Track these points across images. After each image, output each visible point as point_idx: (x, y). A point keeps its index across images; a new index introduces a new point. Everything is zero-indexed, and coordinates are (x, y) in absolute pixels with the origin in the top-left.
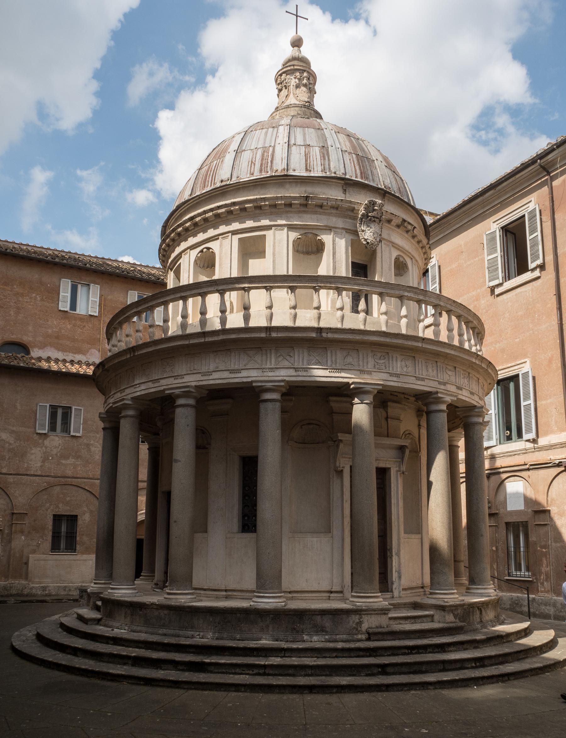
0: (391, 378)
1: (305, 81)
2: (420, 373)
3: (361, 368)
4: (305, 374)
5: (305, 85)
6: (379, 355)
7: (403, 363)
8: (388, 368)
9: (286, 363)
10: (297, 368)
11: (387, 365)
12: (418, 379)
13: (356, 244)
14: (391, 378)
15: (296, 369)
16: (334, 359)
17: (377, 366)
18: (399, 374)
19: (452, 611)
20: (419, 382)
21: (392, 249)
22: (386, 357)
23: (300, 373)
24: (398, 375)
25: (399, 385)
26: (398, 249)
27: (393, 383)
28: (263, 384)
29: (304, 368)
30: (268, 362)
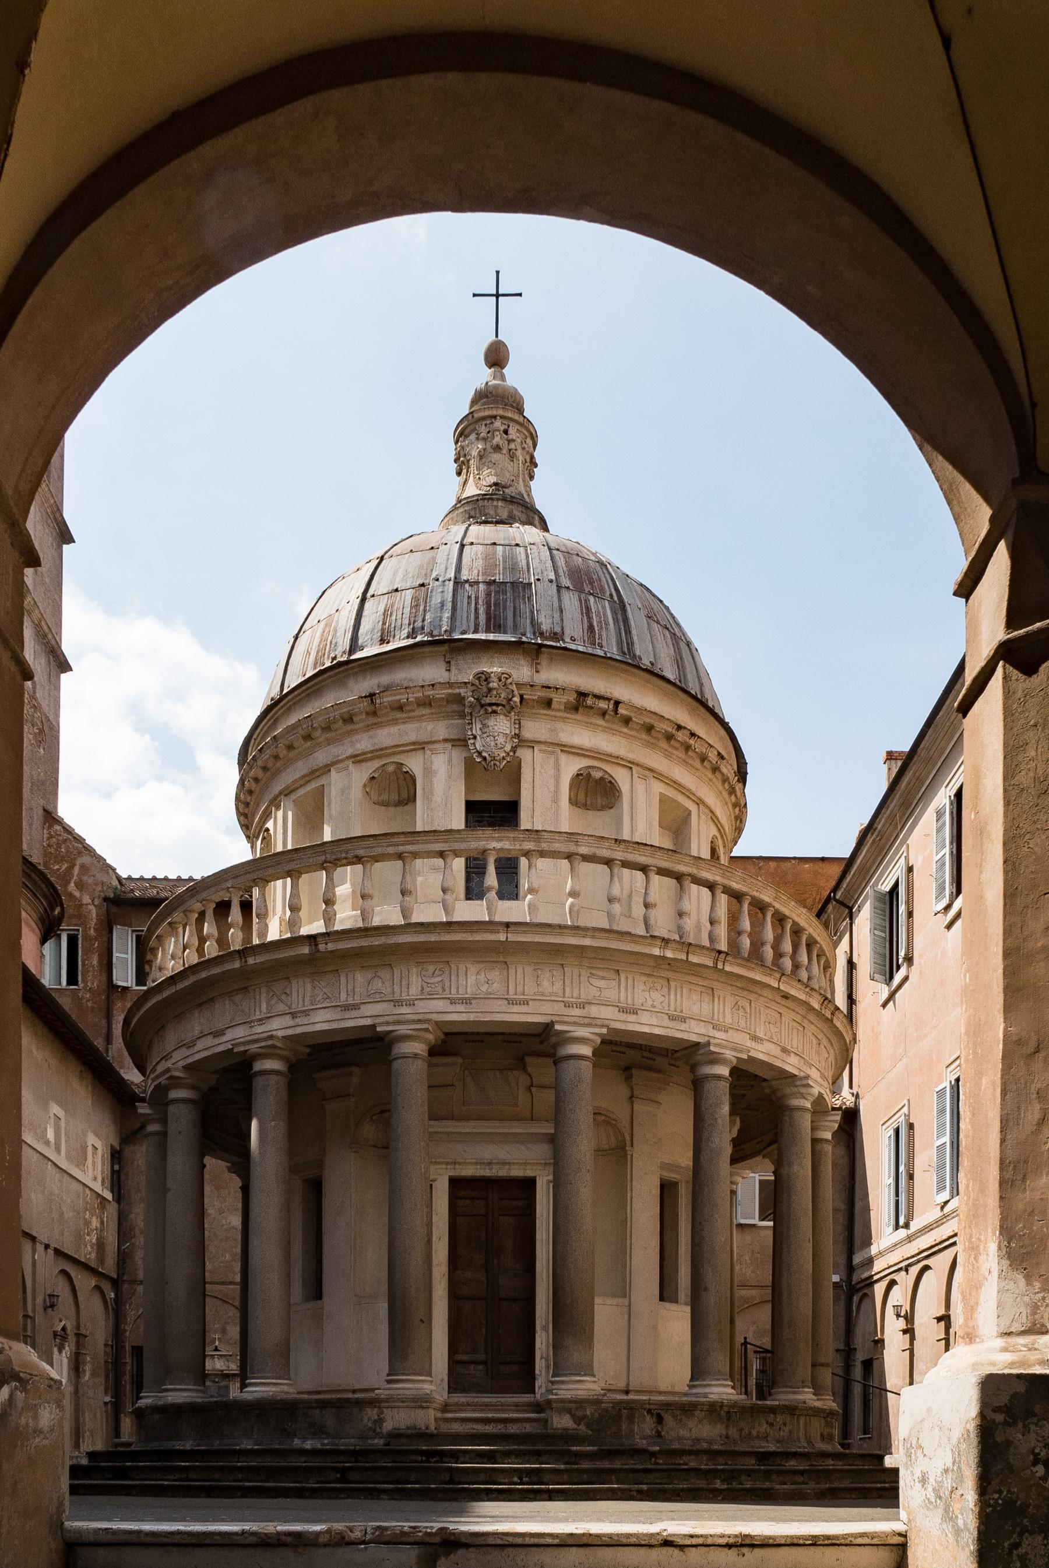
0: (452, 1008)
1: (497, 440)
2: (520, 989)
3: (397, 996)
4: (305, 1021)
5: (497, 448)
6: (431, 968)
7: (482, 977)
8: (447, 991)
9: (281, 1007)
10: (296, 1013)
11: (447, 985)
12: (511, 1002)
13: (476, 768)
14: (452, 1008)
15: (294, 1015)
16: (350, 988)
17: (427, 990)
18: (470, 999)
19: (569, 1411)
20: (516, 1009)
21: (564, 758)
22: (447, 969)
23: (299, 1021)
24: (467, 1001)
25: (472, 1017)
26: (584, 755)
27: (458, 1015)
28: (247, 1048)
29: (304, 1011)
30: (257, 1010)
